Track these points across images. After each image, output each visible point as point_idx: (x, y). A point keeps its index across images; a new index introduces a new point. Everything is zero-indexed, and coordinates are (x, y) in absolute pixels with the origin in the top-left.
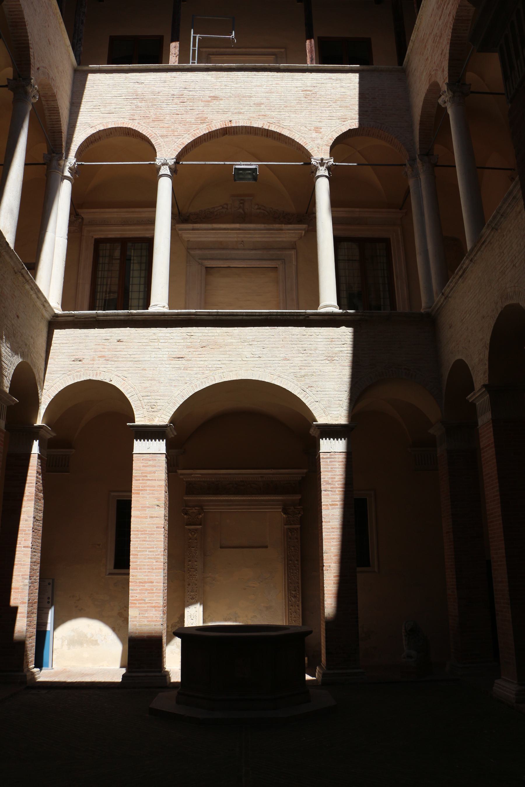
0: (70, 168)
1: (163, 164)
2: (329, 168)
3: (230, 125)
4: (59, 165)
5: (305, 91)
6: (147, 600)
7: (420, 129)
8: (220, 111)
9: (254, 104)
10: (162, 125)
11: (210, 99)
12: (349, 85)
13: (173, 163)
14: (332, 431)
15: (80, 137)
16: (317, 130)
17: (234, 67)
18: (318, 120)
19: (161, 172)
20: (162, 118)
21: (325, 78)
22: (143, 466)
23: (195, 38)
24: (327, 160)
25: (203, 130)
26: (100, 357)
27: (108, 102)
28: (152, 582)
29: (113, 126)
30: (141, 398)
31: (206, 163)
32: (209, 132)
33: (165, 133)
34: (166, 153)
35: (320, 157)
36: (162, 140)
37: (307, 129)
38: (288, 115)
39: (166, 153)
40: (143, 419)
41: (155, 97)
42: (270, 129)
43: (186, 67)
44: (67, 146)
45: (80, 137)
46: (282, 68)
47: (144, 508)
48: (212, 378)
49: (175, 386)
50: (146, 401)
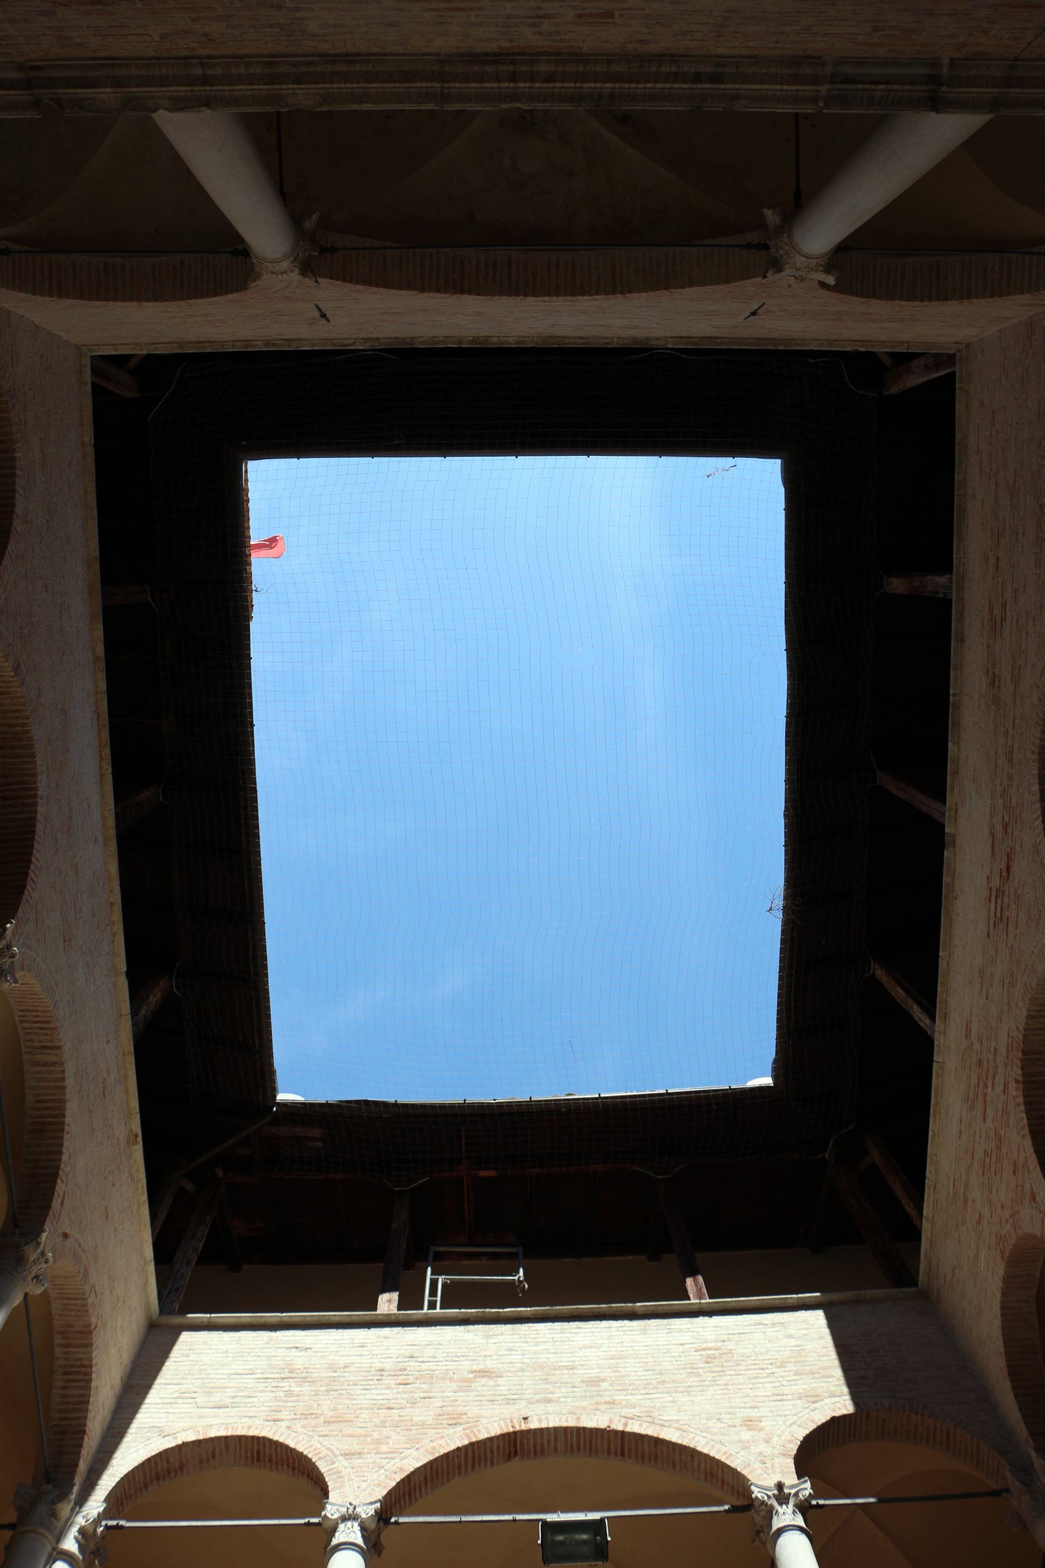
0: (82, 1531)
1: (344, 1519)
2: (804, 1508)
3: (524, 1427)
4: (54, 1515)
5: (704, 1349)
7: (1014, 1388)
8: (499, 1398)
9: (583, 1382)
10: (350, 1431)
11: (471, 1376)
12: (805, 1332)
13: (372, 1512)
15: (127, 1458)
17: (528, 1314)
18: (749, 1405)
19: (339, 1538)
20: (350, 1417)
21: (745, 1323)
23: (434, 1283)
24: (792, 1487)
27: (218, 1385)
29: (223, 1433)
31: (464, 1519)
32: (472, 1444)
33: (356, 1448)
35: (771, 1482)
36: (345, 1463)
37: (723, 1425)
38: (671, 1399)
41: (335, 1374)
42: (628, 1429)
43: (415, 1318)
44: (88, 1478)
45: (127, 1458)
46: (640, 1311)
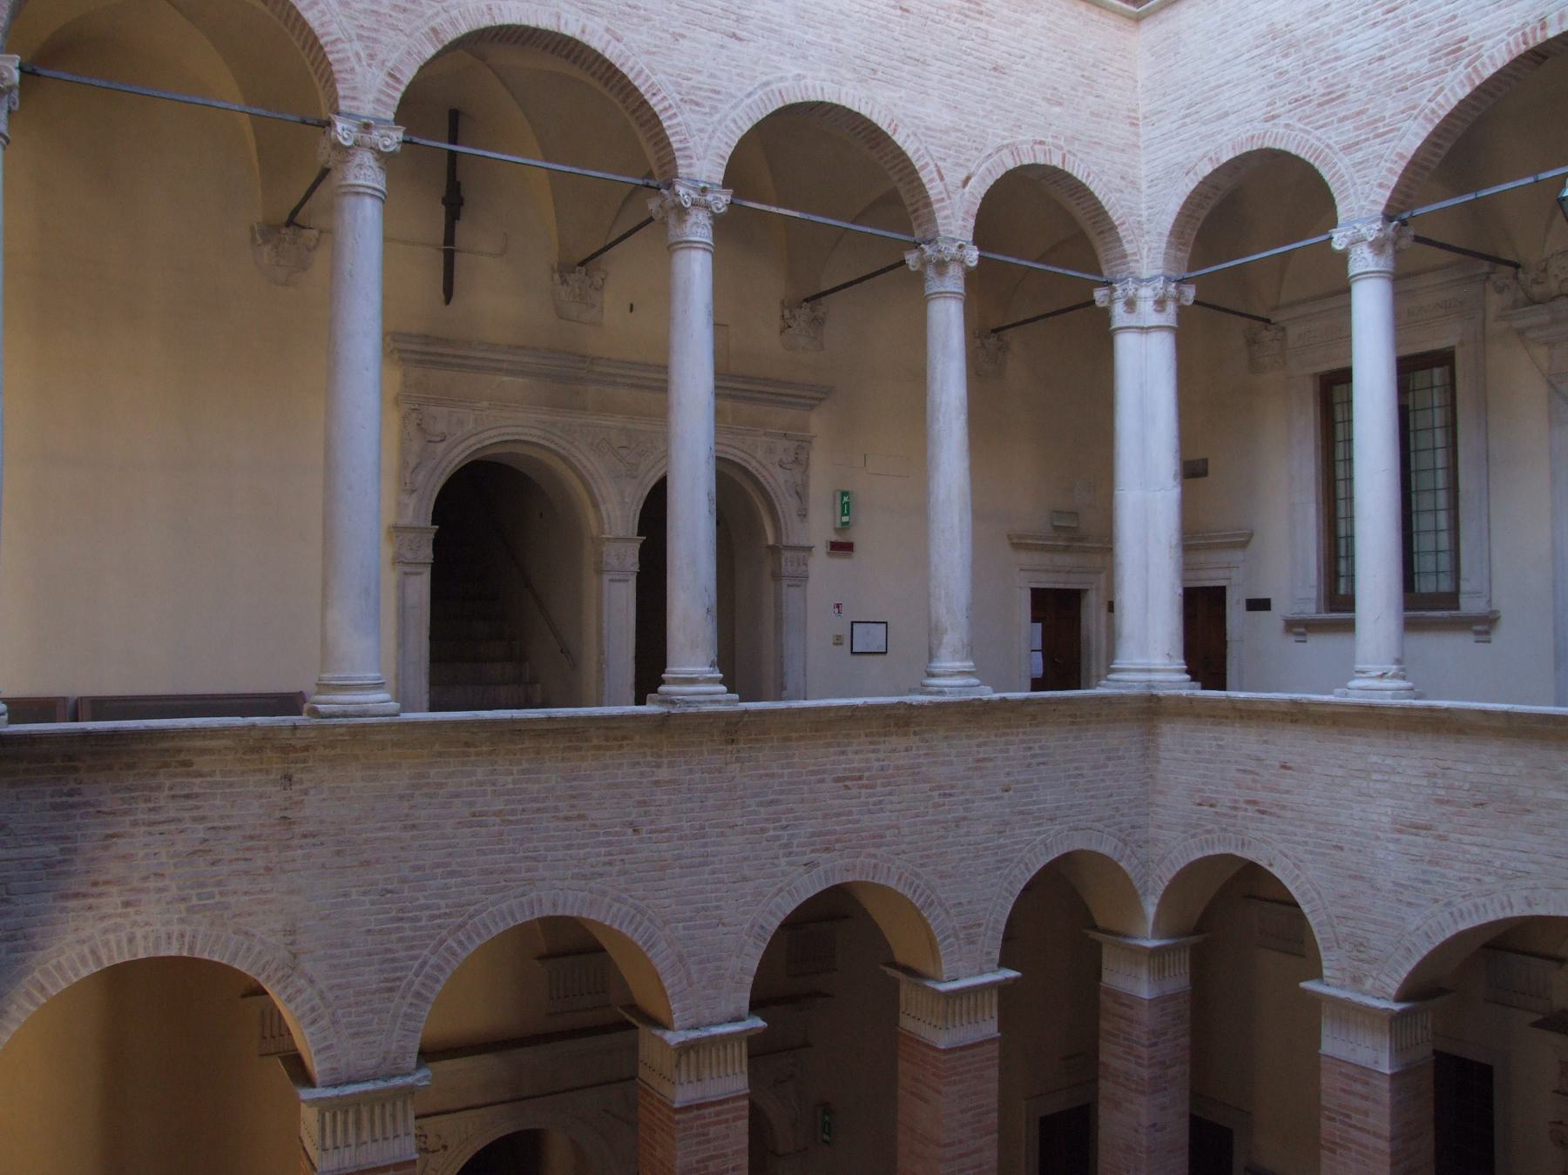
19: (1355, 268)
22: (1343, 1090)
26: (1248, 802)
36: (1346, 160)
40: (1338, 974)
48: (1505, 899)
49: (1409, 904)
50: (1345, 930)
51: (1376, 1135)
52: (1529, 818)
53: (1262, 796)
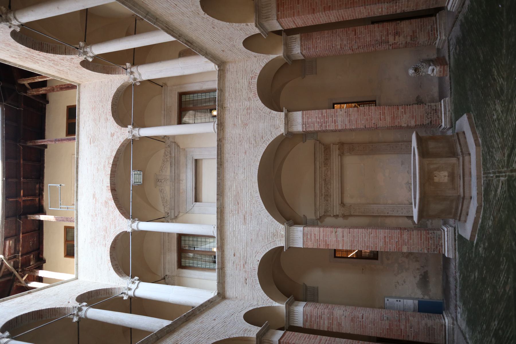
6: (396, 240)
14: (288, 122)
16: (112, 135)
19: (136, 228)
25: (112, 203)
28: (385, 237)
29: (109, 257)
30: (269, 242)
34: (126, 225)
39: (126, 225)
47: (337, 241)
51: (320, 232)
52: (240, 192)
53: (242, 263)
